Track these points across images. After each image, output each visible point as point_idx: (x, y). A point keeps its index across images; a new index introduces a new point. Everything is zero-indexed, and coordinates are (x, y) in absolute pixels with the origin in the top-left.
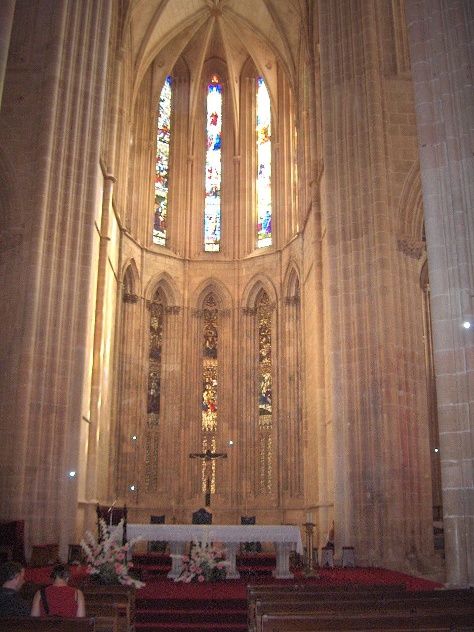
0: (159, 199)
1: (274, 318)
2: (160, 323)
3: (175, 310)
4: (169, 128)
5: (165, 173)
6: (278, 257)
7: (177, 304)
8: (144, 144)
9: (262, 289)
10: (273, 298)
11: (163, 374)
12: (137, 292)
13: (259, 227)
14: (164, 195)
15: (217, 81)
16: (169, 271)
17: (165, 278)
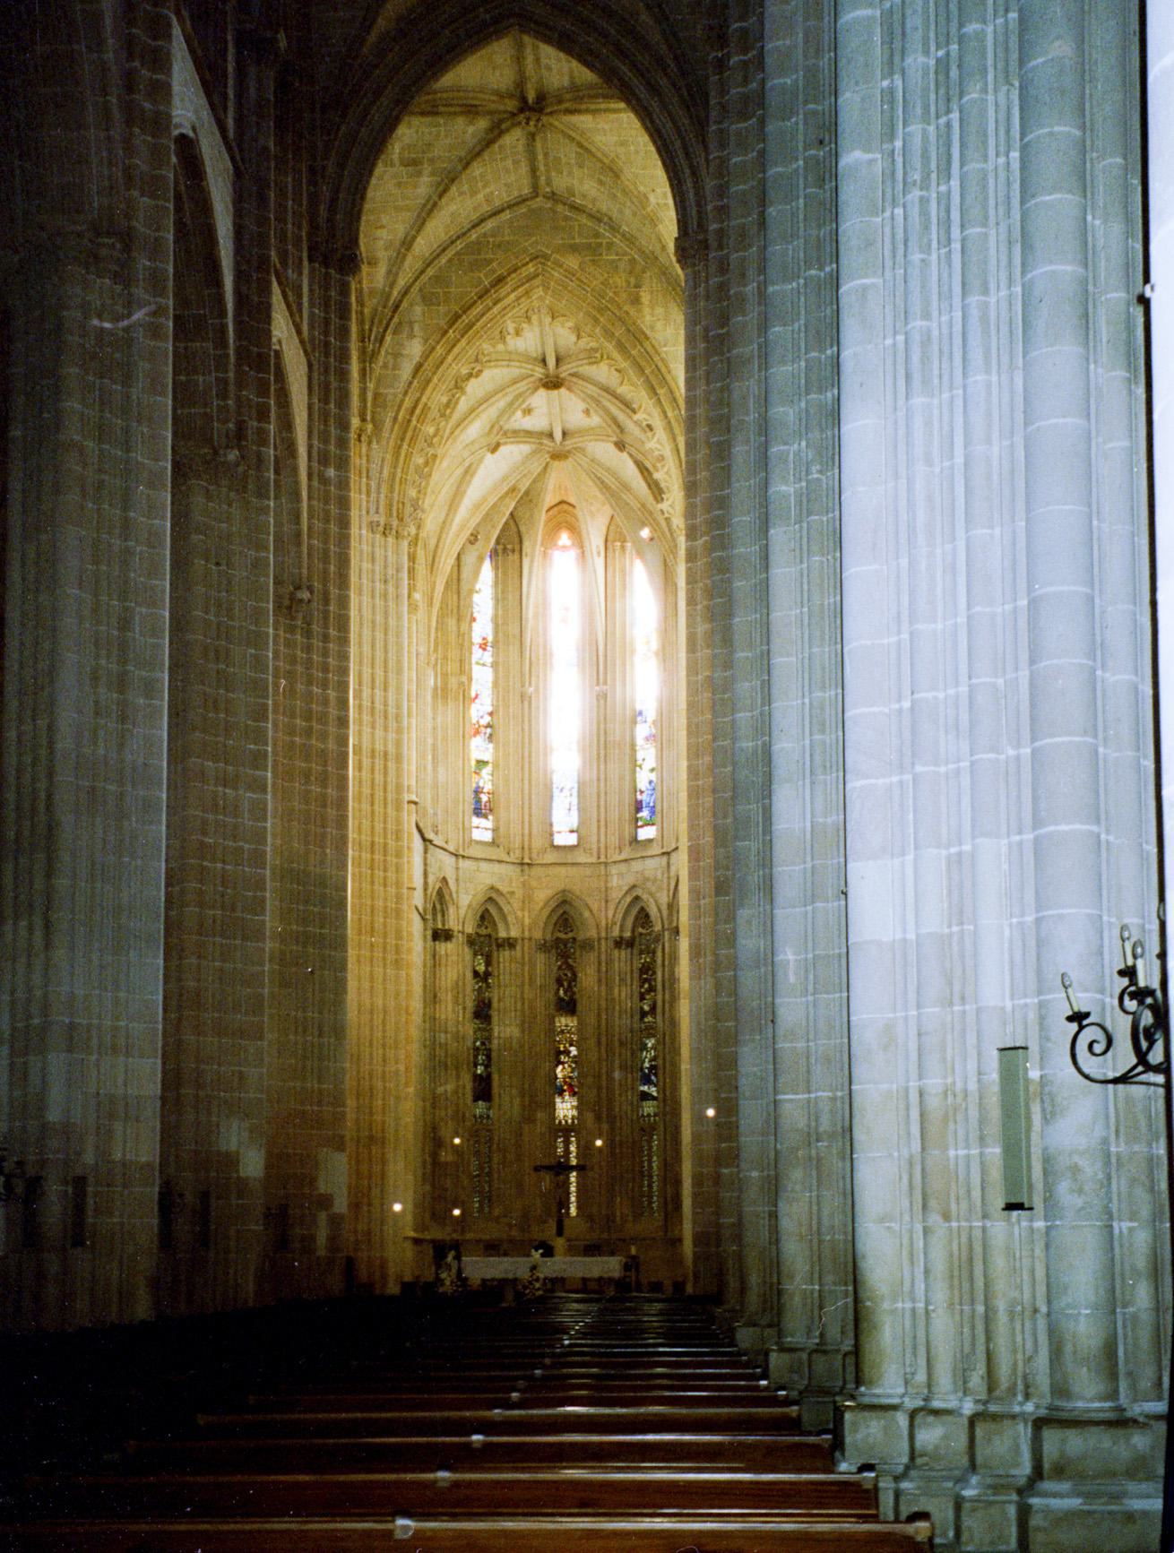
0: (481, 763)
1: (659, 954)
2: (488, 963)
3: (510, 943)
4: (490, 639)
5: (487, 719)
6: (665, 858)
7: (514, 933)
8: (453, 682)
9: (642, 909)
10: (658, 927)
11: (495, 1042)
12: (453, 923)
13: (639, 807)
14: (487, 756)
15: (568, 543)
16: (499, 886)
17: (494, 895)
